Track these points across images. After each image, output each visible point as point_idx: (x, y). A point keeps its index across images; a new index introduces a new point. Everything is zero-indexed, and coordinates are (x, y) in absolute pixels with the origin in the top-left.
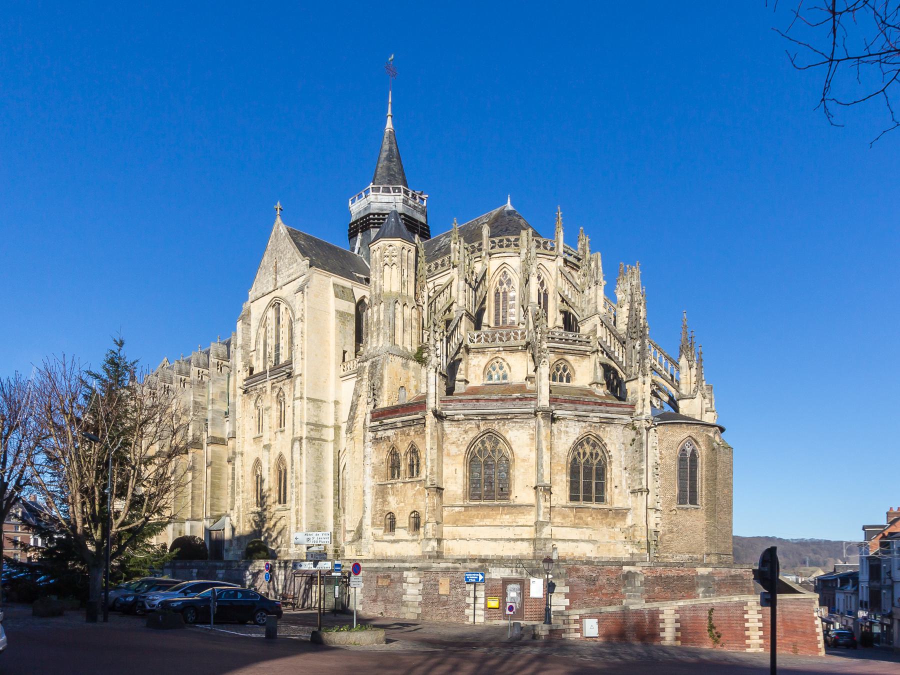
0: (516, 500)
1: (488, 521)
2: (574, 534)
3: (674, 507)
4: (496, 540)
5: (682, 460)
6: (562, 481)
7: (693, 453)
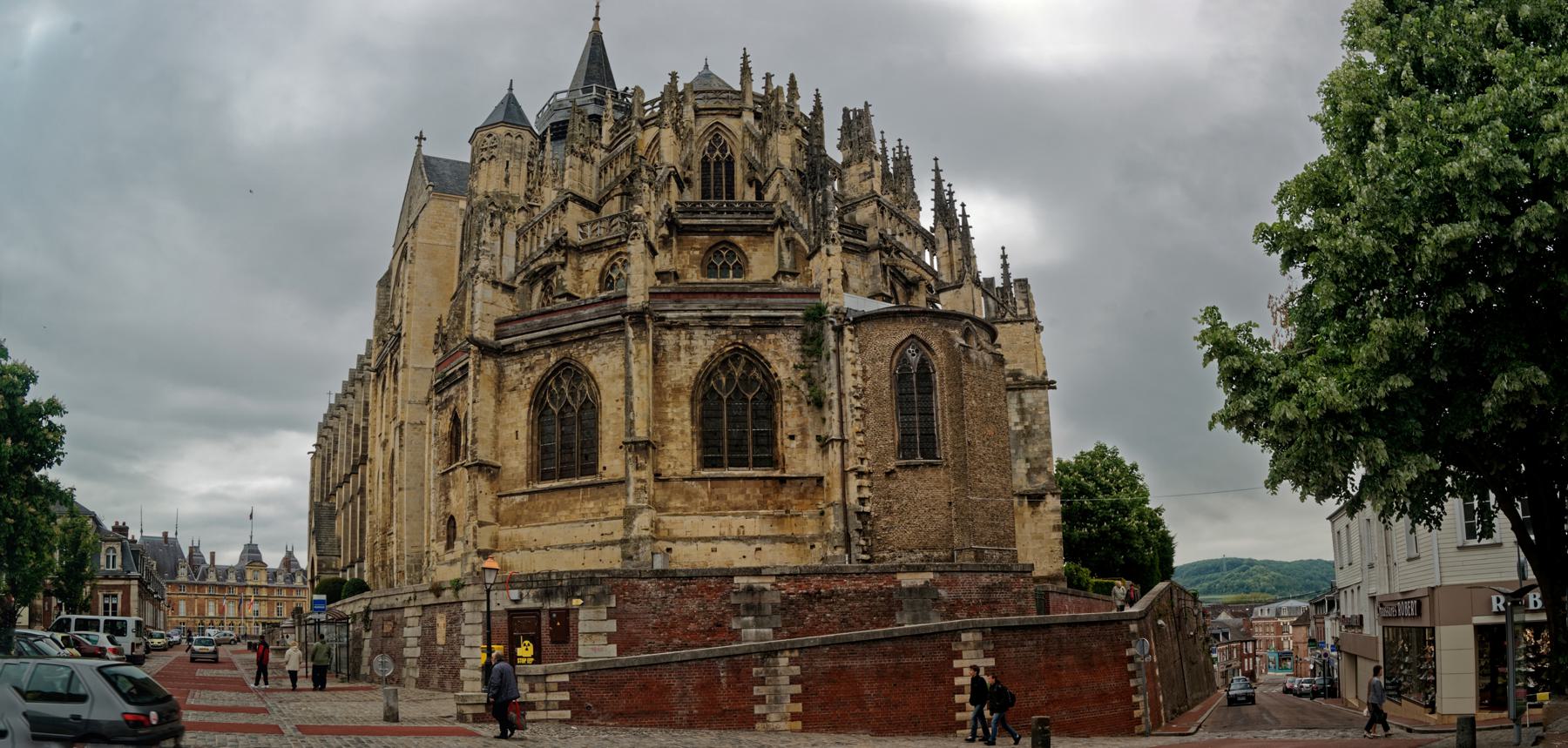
1: (563, 514)
2: (709, 526)
3: (891, 466)
4: (573, 547)
5: (901, 378)
6: (682, 432)
7: (923, 363)
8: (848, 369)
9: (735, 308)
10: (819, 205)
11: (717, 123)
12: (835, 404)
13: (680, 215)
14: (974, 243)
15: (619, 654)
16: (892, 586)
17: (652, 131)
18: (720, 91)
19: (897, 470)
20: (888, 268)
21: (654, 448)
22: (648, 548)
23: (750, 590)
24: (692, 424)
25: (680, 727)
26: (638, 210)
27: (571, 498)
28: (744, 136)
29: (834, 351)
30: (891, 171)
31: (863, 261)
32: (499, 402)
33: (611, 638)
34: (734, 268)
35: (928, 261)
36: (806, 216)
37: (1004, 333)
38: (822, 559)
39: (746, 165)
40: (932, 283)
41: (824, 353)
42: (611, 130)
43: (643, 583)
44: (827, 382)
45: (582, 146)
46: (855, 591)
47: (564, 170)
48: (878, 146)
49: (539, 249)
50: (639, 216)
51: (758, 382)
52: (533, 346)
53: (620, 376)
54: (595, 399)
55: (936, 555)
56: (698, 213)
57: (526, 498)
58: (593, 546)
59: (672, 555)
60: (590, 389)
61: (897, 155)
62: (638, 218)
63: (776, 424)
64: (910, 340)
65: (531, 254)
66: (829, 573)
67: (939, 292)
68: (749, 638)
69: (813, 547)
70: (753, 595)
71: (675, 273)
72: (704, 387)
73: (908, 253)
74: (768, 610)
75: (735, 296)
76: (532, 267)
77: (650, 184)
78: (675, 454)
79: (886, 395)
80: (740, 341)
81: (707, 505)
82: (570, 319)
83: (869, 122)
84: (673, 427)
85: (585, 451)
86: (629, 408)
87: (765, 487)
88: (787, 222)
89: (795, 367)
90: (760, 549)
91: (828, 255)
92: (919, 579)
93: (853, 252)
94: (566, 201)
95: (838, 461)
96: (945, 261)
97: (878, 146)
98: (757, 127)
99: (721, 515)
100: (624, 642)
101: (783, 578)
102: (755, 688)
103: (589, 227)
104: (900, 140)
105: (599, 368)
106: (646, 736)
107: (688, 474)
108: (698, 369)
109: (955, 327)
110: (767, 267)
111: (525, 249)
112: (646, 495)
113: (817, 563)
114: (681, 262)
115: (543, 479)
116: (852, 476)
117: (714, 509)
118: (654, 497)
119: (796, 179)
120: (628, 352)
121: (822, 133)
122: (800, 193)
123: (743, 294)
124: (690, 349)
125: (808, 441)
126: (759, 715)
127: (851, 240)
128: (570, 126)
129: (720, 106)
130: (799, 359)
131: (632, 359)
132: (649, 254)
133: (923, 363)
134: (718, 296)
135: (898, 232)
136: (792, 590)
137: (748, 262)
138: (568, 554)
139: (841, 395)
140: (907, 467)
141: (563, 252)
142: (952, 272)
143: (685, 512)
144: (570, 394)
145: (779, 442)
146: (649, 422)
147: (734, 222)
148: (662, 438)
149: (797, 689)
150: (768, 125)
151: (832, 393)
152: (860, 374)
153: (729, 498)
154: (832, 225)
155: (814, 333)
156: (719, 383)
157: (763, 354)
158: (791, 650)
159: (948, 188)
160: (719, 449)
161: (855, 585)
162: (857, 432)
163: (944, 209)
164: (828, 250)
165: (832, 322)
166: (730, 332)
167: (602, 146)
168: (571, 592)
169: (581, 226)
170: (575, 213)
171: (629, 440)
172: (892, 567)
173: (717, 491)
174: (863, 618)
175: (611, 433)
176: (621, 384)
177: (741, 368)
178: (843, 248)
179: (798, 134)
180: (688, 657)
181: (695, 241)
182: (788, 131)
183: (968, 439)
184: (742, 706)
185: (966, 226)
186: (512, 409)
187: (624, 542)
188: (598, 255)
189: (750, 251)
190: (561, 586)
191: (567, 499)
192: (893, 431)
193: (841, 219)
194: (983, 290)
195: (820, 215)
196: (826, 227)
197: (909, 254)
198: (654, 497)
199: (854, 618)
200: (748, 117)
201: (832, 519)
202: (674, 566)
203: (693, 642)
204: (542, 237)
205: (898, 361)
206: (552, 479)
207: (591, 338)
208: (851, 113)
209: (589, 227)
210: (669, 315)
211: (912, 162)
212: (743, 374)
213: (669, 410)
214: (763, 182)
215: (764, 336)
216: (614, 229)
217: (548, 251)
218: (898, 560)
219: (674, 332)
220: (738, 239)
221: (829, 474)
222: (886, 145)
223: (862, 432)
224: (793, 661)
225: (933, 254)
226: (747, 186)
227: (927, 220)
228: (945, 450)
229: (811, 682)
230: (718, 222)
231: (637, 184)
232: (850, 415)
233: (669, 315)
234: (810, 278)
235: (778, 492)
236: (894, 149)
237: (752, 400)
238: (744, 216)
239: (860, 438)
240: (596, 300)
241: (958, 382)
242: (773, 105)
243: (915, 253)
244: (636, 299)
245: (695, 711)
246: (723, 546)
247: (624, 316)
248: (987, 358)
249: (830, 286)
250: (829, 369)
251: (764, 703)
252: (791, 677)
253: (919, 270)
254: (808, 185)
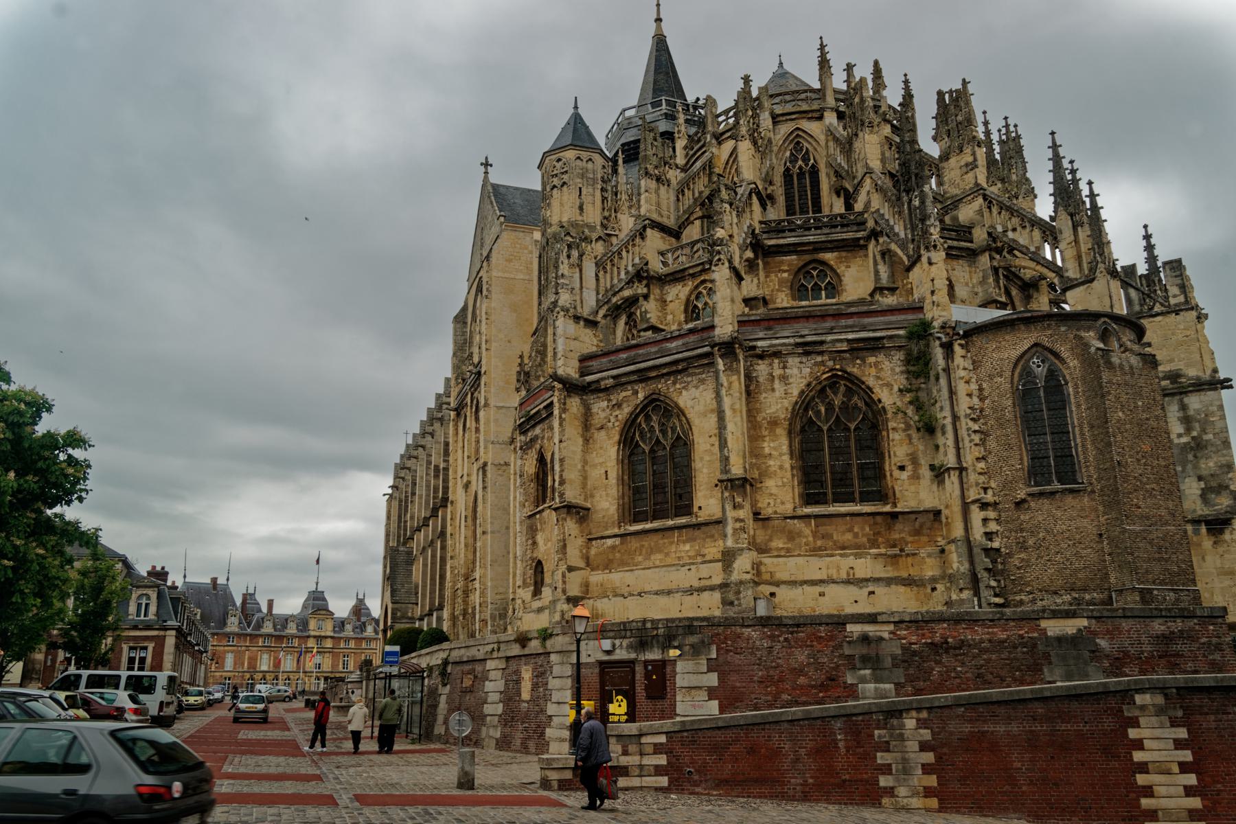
0: (700, 513)
1: (657, 558)
2: (814, 568)
3: (1021, 495)
4: (669, 592)
5: (1025, 395)
6: (781, 467)
7: (1052, 374)
8: (962, 389)
9: (831, 331)
10: (916, 208)
11: (798, 129)
12: (949, 428)
13: (765, 236)
14: (1108, 227)
15: (722, 711)
16: (1036, 635)
17: (728, 146)
18: (797, 92)
19: (1029, 499)
20: (1001, 271)
21: (752, 485)
22: (750, 592)
23: (865, 639)
24: (791, 458)
25: (792, 799)
26: (720, 233)
28: (827, 141)
29: (944, 370)
30: (998, 157)
31: (970, 266)
33: (712, 693)
34: (826, 289)
35: (1048, 256)
36: (902, 223)
37: (1154, 329)
38: (946, 603)
39: (832, 173)
40: (1056, 281)
41: (932, 373)
42: (685, 148)
43: (747, 631)
44: (938, 405)
45: (656, 167)
46: (990, 641)
47: (639, 194)
48: (981, 129)
49: (620, 280)
50: (722, 240)
51: (860, 410)
52: (620, 383)
53: (712, 411)
54: (686, 435)
55: (1087, 597)
56: (784, 231)
57: (617, 541)
58: (691, 591)
59: (776, 600)
60: (681, 425)
61: (1004, 137)
62: (721, 242)
63: (882, 454)
64: (1035, 349)
65: (612, 286)
66: (957, 620)
67: (1064, 291)
68: (868, 694)
69: (934, 589)
70: (869, 644)
71: (764, 299)
72: (801, 418)
73: (1024, 249)
74: (888, 662)
75: (829, 319)
76: (614, 300)
77: (731, 205)
78: (774, 491)
79: (1008, 415)
80: (838, 367)
81: (812, 545)
82: (656, 352)
83: (968, 103)
84: (771, 463)
85: (679, 491)
86: (723, 444)
87: (876, 523)
88: (881, 232)
89: (900, 390)
90: (873, 593)
91: (930, 263)
92: (1070, 627)
93: (957, 257)
94: (644, 228)
95: (957, 492)
96: (1071, 253)
97: (981, 129)
98: (841, 129)
99: (828, 556)
100: (727, 696)
101: (903, 626)
102: (879, 754)
103: (670, 255)
104: (1006, 118)
105: (689, 403)
106: (754, 809)
107: (790, 512)
108: (794, 399)
109: (1089, 329)
110: (861, 284)
111: (606, 282)
112: (746, 536)
113: (940, 608)
114: (769, 286)
115: (636, 519)
116: (975, 509)
117: (820, 549)
118: (754, 536)
119: (888, 183)
120: (719, 385)
121: (914, 125)
122: (894, 198)
123: (838, 315)
124: (784, 378)
125: (921, 472)
126: (885, 788)
127: (955, 243)
128: (642, 146)
129: (798, 109)
130: (905, 382)
131: (723, 392)
132: (734, 280)
133: (1052, 374)
134: (811, 319)
135: (1010, 227)
136: (914, 639)
137: (841, 281)
138: (663, 601)
139: (955, 418)
140: (1041, 494)
141: (645, 282)
142: (1080, 265)
143: (788, 553)
144: (661, 431)
145: (888, 474)
146: (744, 457)
147: (823, 238)
148: (760, 475)
149: (929, 757)
150: (853, 125)
151: (945, 418)
152: (976, 393)
153: (835, 538)
154: (932, 230)
155: (919, 352)
156: (818, 413)
157: (864, 379)
158: (919, 710)
159: (1069, 166)
160: (822, 484)
161: (988, 633)
162: (978, 459)
163: (1066, 192)
164: (929, 259)
165: (939, 338)
166: (826, 358)
167: (677, 167)
168: (668, 641)
169: (662, 254)
170: (655, 240)
171: (725, 477)
172: (1033, 611)
173: (822, 529)
174: (1003, 673)
175: (705, 471)
176: (713, 419)
177: (840, 396)
178: (947, 254)
179: (887, 130)
180: (800, 716)
181: (782, 262)
182: (876, 129)
183: (1116, 458)
184: (865, 776)
185: (1095, 208)
186: (601, 448)
187: (724, 586)
188: (681, 284)
189: (843, 268)
190: (657, 635)
191: (661, 542)
192: (1021, 455)
193: (942, 221)
194: (1122, 281)
195: (918, 220)
196: (926, 233)
197: (1025, 251)
198: (754, 536)
199: (992, 674)
200: (831, 118)
201: (954, 557)
202: (779, 613)
203: (804, 699)
204: (622, 268)
205: (1021, 376)
206: (645, 520)
207: (680, 372)
208: (947, 96)
209: (670, 255)
210: (759, 344)
211: (1022, 142)
212: (843, 402)
213: (765, 444)
214: (851, 191)
215: (863, 360)
216: (696, 255)
217: (630, 282)
218: (1040, 603)
219: (766, 362)
220: (829, 257)
221: (947, 507)
222: (990, 127)
223: (983, 458)
224: (921, 724)
225: (1054, 247)
226: (834, 197)
227: (1044, 208)
228: (1088, 472)
229: (945, 750)
230: (805, 239)
231: (716, 205)
232: (967, 439)
233: (759, 344)
234: (911, 292)
235: (890, 528)
236: (999, 131)
237: (855, 430)
238: (833, 230)
239: (982, 465)
240: (682, 332)
241: (1098, 393)
242: (857, 100)
243: (1032, 249)
244: (725, 328)
245: (811, 781)
246: (831, 590)
247: (712, 347)
248: (1134, 361)
249: (935, 298)
250: (939, 391)
251: (890, 774)
252: (920, 742)
253: (1039, 268)
254: (902, 188)
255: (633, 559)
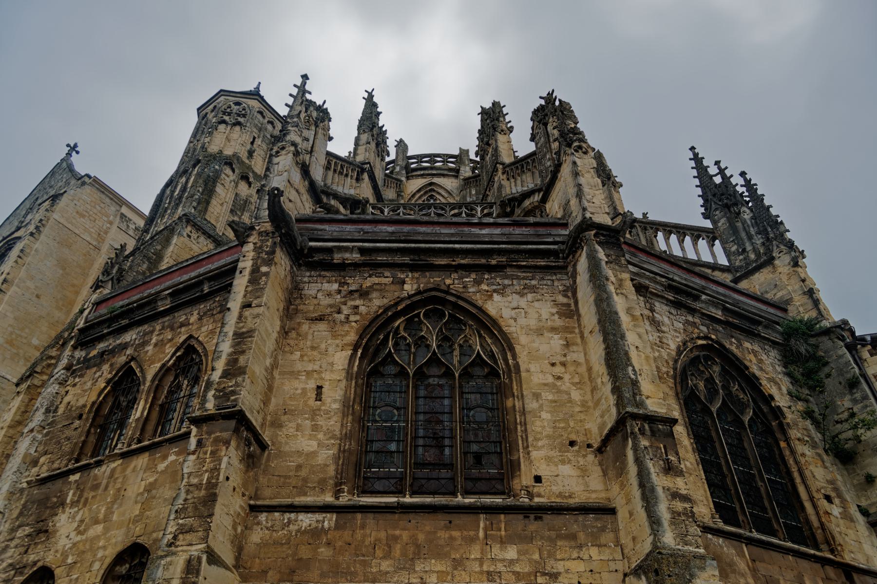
27: (456, 534)
32: (285, 333)
105: (507, 313)
186: (313, 348)
191: (443, 535)
207: (490, 269)
255: (365, 564)
